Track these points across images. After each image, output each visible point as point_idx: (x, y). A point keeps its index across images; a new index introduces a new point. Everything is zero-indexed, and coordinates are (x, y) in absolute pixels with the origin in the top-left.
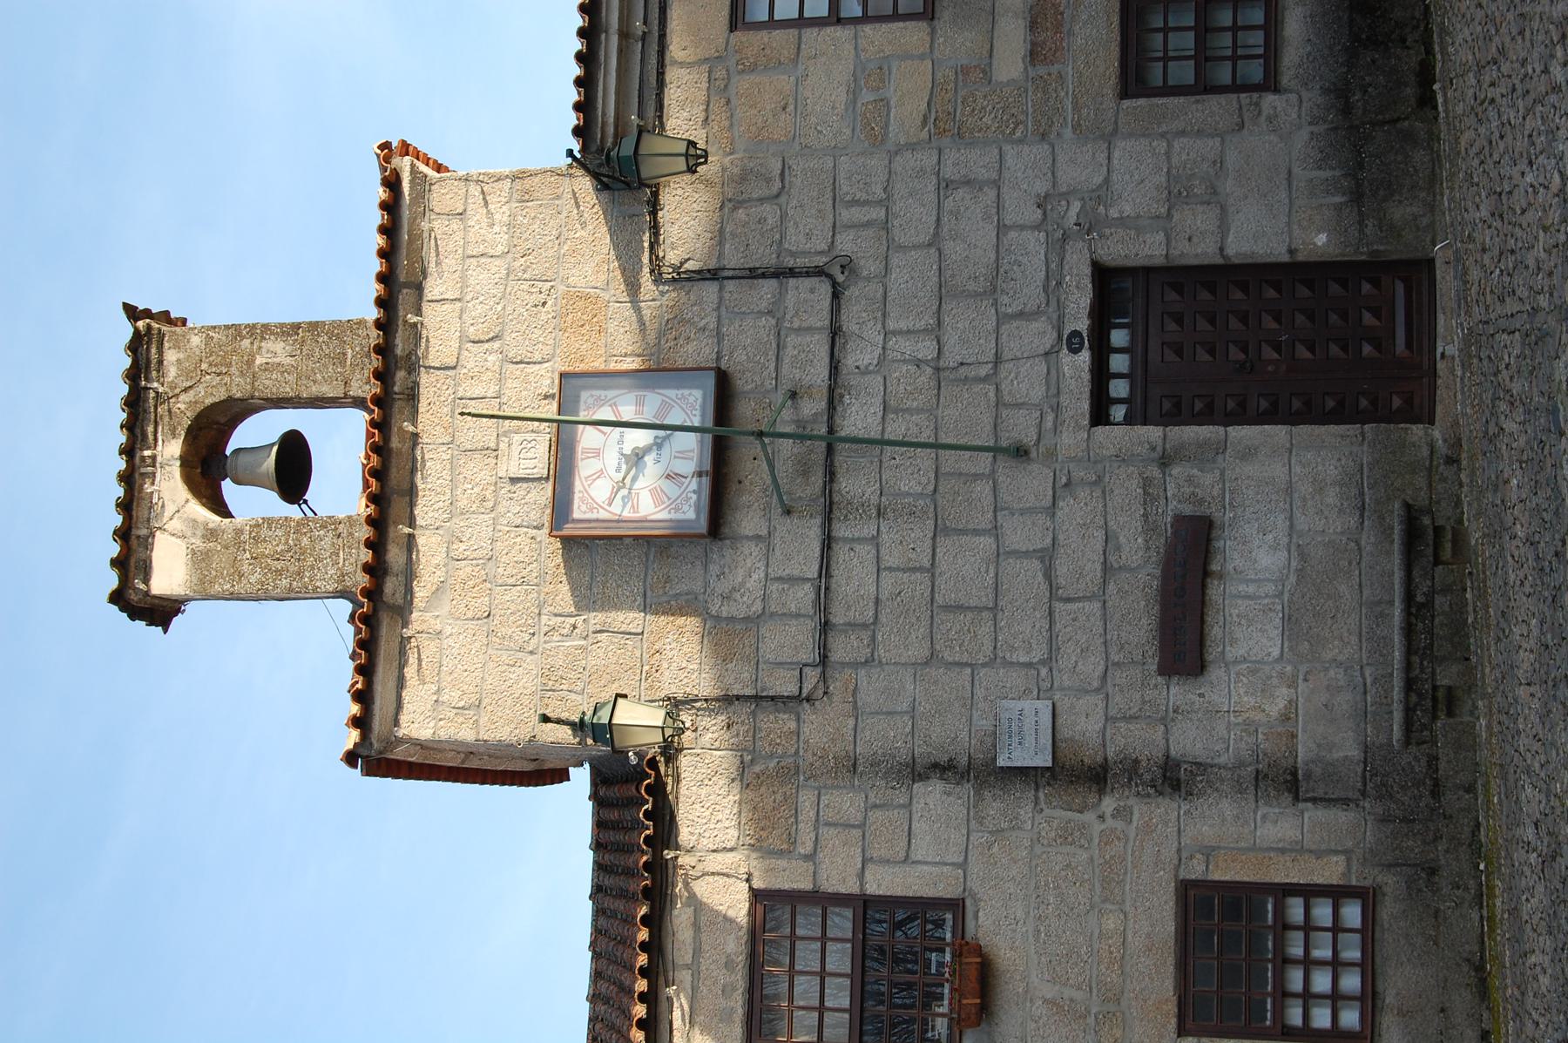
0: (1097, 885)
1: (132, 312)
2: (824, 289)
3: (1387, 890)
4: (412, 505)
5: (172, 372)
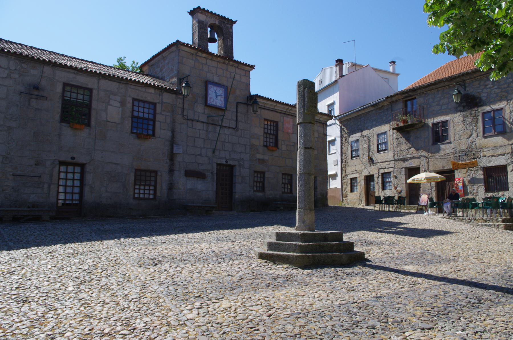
1: (236, 21)
2: (234, 127)
4: (210, 60)
5: (227, 25)
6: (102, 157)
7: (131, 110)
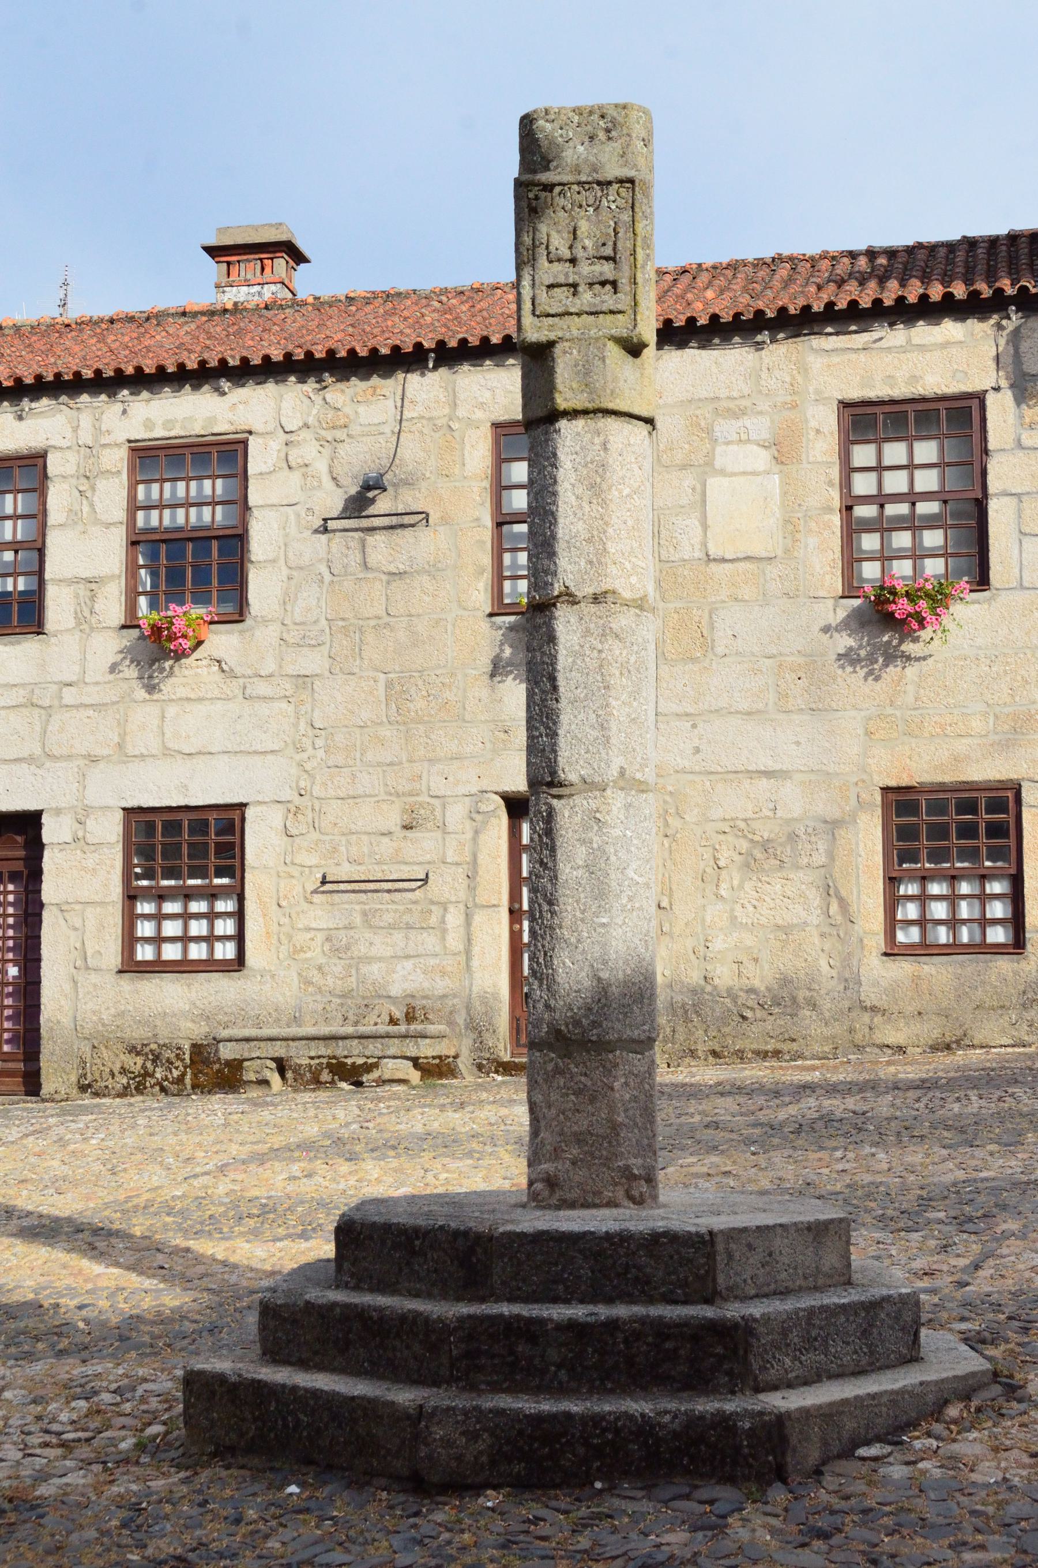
0: (1010, 709)
3: (1023, 964)
6: (697, 750)
7: (835, 473)
